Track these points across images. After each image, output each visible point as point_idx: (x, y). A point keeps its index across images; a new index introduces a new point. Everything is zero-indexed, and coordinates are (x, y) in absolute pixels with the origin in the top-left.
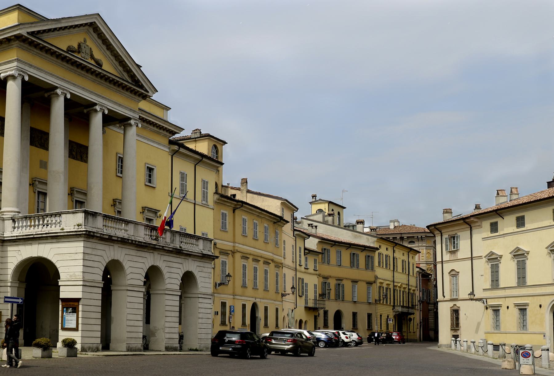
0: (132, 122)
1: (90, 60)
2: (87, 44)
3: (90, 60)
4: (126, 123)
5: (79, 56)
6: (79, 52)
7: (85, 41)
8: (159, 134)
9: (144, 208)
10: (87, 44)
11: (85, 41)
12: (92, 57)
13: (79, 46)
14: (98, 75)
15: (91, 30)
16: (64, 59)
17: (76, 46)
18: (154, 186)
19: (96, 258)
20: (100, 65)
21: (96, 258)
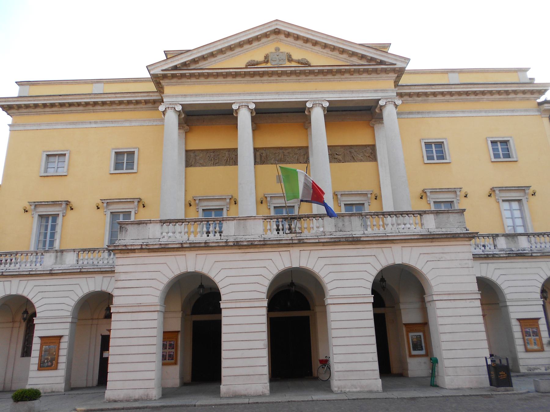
0: (381, 103)
1: (288, 64)
2: (281, 51)
3: (288, 64)
4: (378, 106)
5: (269, 65)
6: (267, 62)
7: (277, 49)
8: (513, 99)
9: (493, 190)
10: (281, 51)
11: (277, 49)
12: (290, 59)
13: (266, 57)
14: (312, 72)
15: (282, 37)
16: (246, 74)
17: (261, 58)
18: (515, 160)
19: (154, 275)
20: (307, 64)
21: (154, 275)
